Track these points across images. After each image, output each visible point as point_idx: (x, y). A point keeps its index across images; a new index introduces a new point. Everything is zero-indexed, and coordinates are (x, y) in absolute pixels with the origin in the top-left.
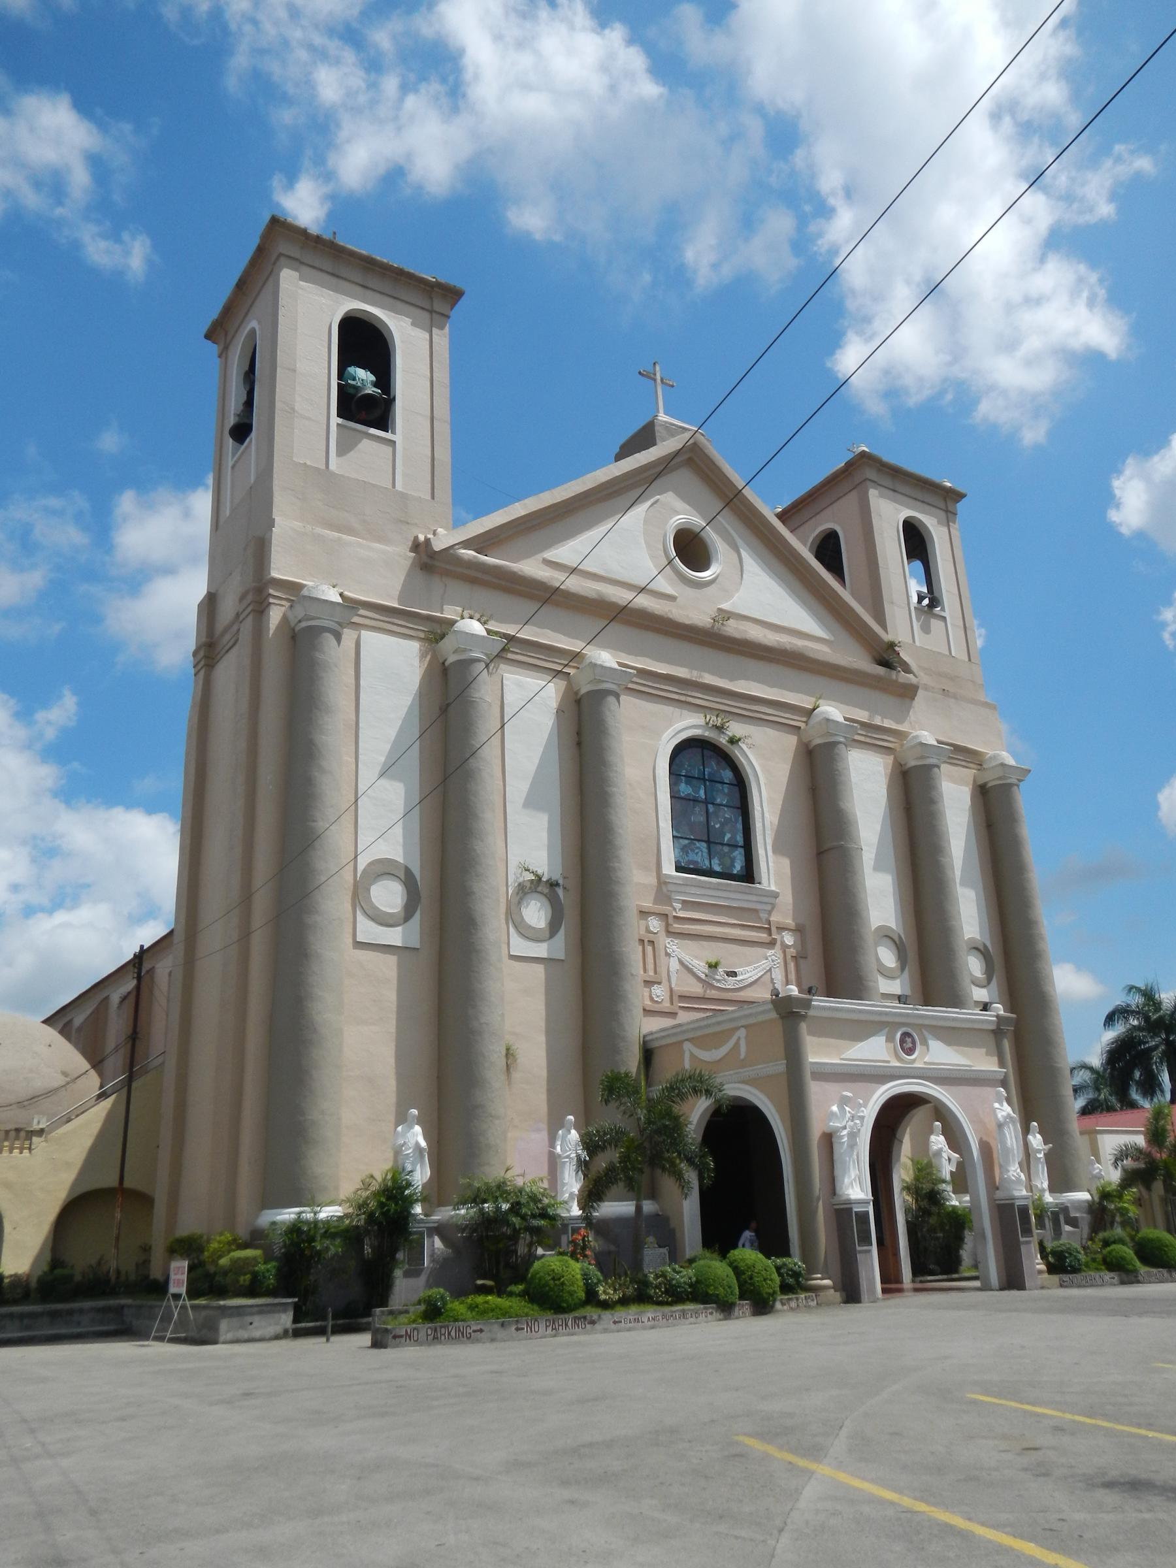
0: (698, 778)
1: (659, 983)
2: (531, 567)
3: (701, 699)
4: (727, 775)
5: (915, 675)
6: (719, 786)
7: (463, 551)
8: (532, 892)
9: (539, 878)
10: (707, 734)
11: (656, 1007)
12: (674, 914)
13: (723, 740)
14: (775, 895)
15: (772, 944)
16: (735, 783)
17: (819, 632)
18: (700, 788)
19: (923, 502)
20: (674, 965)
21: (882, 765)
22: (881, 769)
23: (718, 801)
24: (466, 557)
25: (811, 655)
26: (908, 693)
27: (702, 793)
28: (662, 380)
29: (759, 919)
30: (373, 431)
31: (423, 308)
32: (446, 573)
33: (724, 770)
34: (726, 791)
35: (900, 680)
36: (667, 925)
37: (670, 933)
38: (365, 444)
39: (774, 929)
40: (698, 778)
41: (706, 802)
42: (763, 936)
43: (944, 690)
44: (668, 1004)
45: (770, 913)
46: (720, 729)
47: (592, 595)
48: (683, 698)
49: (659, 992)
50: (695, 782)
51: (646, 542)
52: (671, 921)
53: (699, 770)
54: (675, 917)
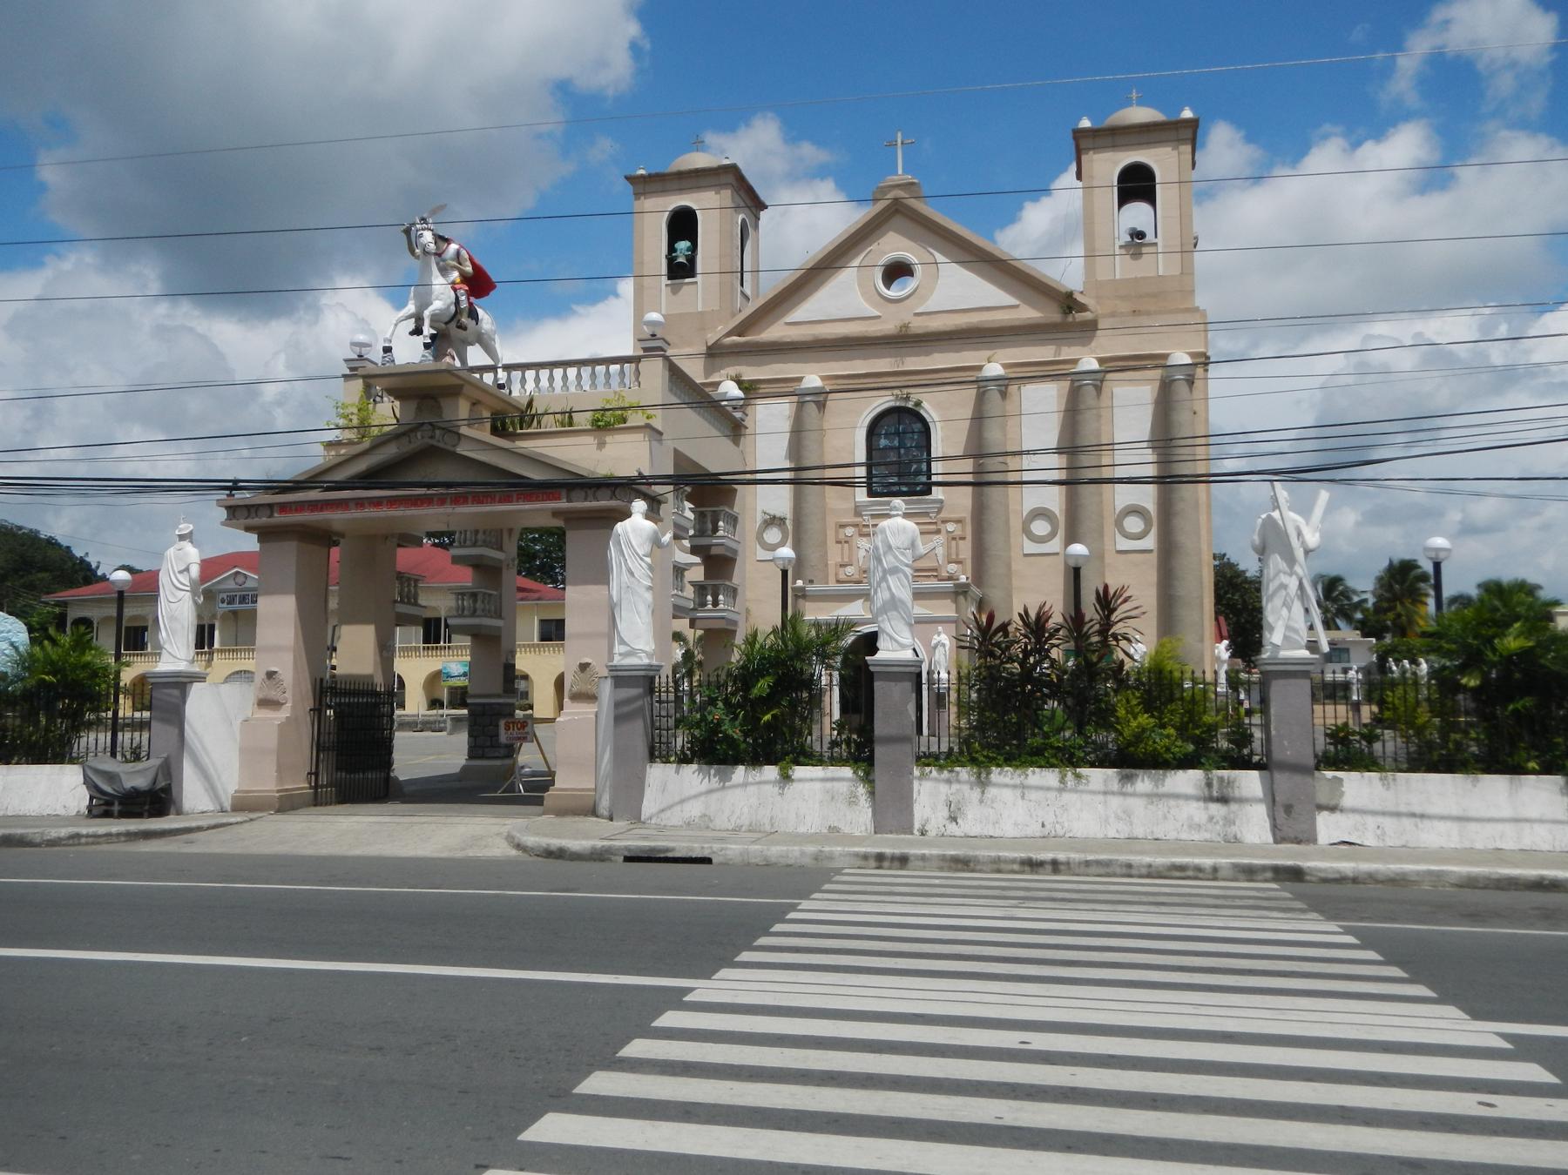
0: (893, 434)
1: (851, 565)
2: (775, 332)
3: (892, 381)
4: (918, 426)
5: (1092, 312)
6: (911, 435)
7: (728, 339)
8: (772, 524)
9: (774, 517)
10: (898, 404)
11: (849, 579)
12: (864, 523)
13: (910, 405)
14: (941, 501)
15: (938, 532)
16: (923, 430)
17: (1009, 300)
18: (894, 440)
19: (1148, 143)
20: (862, 553)
21: (1055, 389)
22: (1054, 393)
23: (909, 445)
24: (728, 343)
25: (987, 326)
26: (1091, 327)
27: (896, 443)
28: (902, 143)
29: (931, 518)
30: (687, 280)
31: (716, 186)
32: (722, 355)
33: (915, 423)
34: (916, 437)
35: (1077, 320)
36: (859, 531)
37: (861, 535)
38: (685, 288)
39: (939, 522)
40: (893, 434)
41: (898, 448)
42: (933, 527)
43: (1134, 311)
44: (858, 576)
45: (939, 512)
46: (907, 399)
47: (809, 338)
48: (880, 385)
49: (850, 570)
50: (892, 436)
51: (860, 285)
52: (861, 527)
53: (896, 428)
54: (864, 525)
